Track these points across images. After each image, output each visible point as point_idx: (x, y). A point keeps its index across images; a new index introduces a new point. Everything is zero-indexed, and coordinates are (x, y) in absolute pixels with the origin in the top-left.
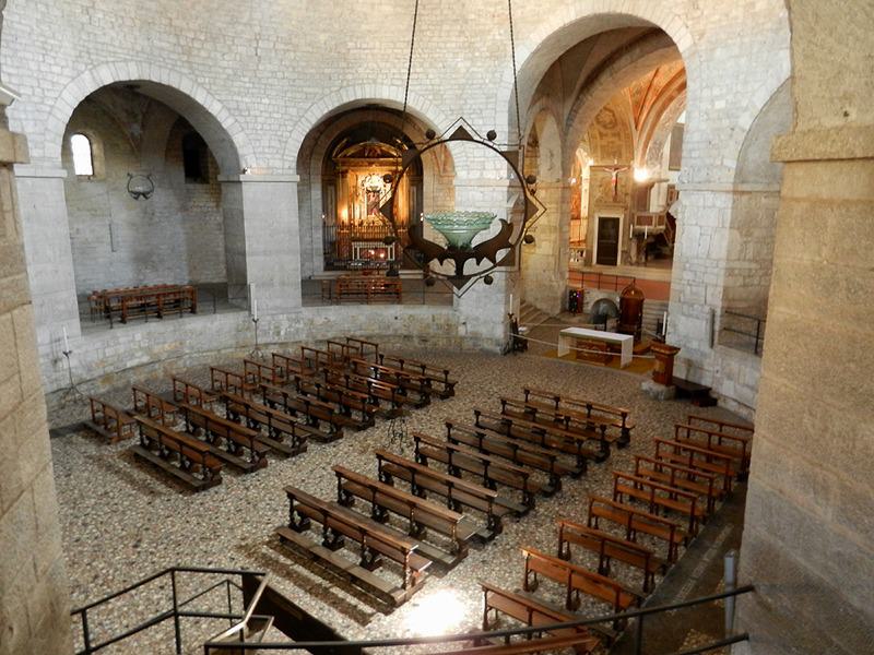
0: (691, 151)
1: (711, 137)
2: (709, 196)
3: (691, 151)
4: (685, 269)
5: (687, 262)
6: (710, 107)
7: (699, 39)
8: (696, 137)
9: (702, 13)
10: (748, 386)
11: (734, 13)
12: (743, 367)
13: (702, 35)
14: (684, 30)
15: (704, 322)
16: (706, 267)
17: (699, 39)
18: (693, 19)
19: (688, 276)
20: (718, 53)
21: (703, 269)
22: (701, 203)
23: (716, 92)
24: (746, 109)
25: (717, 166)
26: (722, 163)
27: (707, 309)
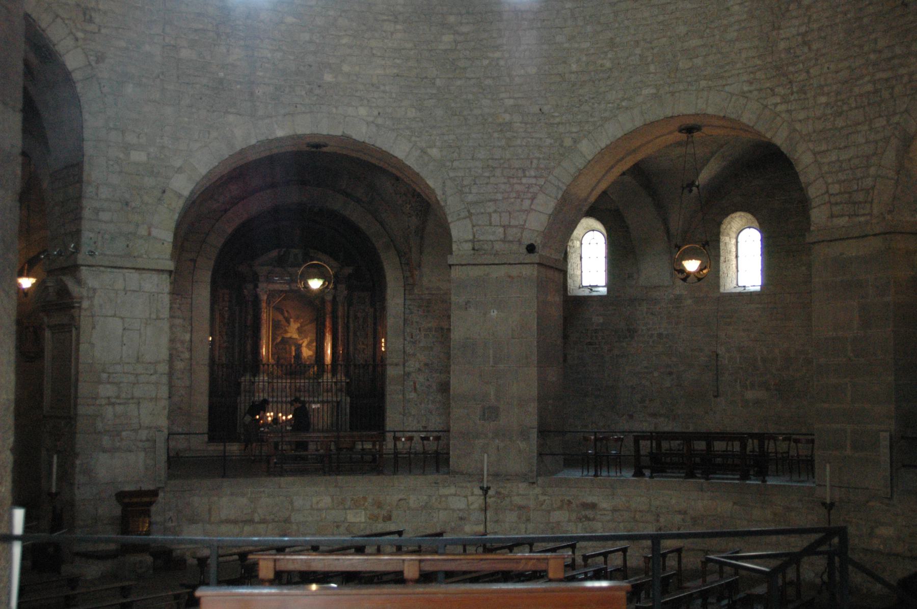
0: (97, 211)
1: (127, 196)
2: (135, 275)
3: (97, 211)
4: (99, 382)
5: (104, 372)
6: (122, 156)
7: (97, 62)
8: (104, 193)
9: (99, 30)
10: (228, 521)
11: (147, 48)
12: (216, 498)
13: (100, 59)
14: (69, 42)
15: (142, 455)
16: (137, 375)
17: (97, 62)
18: (85, 32)
19: (106, 391)
20: (129, 89)
21: (132, 378)
22: (119, 285)
23: (131, 138)
24: (180, 170)
25: (142, 237)
26: (150, 234)
27: (144, 434)
